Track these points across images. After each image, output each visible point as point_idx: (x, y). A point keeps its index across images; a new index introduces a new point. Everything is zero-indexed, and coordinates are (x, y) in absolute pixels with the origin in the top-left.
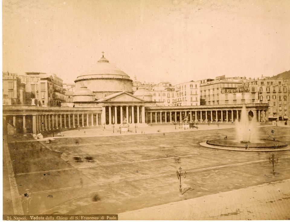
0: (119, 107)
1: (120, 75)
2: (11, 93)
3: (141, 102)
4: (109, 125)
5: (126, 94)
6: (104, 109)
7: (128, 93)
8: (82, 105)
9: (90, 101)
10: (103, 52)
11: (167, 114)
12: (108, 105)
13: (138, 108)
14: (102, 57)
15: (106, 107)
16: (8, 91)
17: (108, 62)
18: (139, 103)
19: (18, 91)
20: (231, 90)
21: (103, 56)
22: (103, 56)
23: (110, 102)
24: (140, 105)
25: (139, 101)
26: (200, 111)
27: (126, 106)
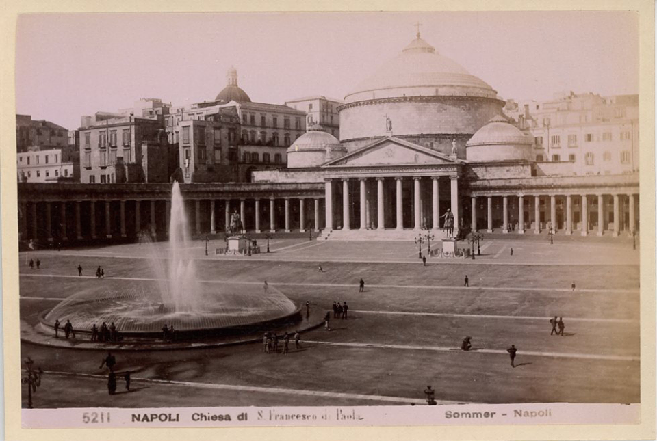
0: (371, 182)
1: (425, 86)
2: (126, 153)
3: (445, 165)
4: (360, 230)
5: (395, 143)
6: (328, 188)
7: (398, 140)
8: (292, 177)
9: (314, 165)
10: (418, 25)
11: (542, 202)
12: (337, 177)
13: (435, 184)
15: (332, 182)
16: (124, 150)
17: (431, 50)
19: (138, 149)
20: (329, 121)
21: (418, 35)
22: (418, 35)
23: (345, 169)
24: (441, 173)
25: (440, 162)
26: (534, 197)
27: (393, 178)
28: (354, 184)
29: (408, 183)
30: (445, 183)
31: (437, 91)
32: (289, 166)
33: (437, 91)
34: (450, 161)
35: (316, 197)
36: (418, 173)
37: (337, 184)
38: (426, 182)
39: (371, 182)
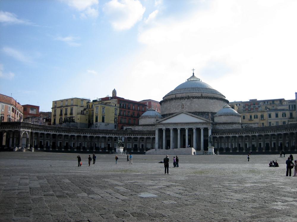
3: (205, 123)
6: (157, 132)
13: (202, 131)
14: (193, 75)
21: (193, 74)
22: (193, 74)
23: (164, 124)
24: (205, 126)
28: (168, 130)
29: (190, 130)
30: (206, 130)
31: (202, 94)
32: (140, 124)
33: (202, 94)
35: (152, 137)
36: (194, 127)
37: (161, 131)
38: (198, 130)
39: (175, 130)
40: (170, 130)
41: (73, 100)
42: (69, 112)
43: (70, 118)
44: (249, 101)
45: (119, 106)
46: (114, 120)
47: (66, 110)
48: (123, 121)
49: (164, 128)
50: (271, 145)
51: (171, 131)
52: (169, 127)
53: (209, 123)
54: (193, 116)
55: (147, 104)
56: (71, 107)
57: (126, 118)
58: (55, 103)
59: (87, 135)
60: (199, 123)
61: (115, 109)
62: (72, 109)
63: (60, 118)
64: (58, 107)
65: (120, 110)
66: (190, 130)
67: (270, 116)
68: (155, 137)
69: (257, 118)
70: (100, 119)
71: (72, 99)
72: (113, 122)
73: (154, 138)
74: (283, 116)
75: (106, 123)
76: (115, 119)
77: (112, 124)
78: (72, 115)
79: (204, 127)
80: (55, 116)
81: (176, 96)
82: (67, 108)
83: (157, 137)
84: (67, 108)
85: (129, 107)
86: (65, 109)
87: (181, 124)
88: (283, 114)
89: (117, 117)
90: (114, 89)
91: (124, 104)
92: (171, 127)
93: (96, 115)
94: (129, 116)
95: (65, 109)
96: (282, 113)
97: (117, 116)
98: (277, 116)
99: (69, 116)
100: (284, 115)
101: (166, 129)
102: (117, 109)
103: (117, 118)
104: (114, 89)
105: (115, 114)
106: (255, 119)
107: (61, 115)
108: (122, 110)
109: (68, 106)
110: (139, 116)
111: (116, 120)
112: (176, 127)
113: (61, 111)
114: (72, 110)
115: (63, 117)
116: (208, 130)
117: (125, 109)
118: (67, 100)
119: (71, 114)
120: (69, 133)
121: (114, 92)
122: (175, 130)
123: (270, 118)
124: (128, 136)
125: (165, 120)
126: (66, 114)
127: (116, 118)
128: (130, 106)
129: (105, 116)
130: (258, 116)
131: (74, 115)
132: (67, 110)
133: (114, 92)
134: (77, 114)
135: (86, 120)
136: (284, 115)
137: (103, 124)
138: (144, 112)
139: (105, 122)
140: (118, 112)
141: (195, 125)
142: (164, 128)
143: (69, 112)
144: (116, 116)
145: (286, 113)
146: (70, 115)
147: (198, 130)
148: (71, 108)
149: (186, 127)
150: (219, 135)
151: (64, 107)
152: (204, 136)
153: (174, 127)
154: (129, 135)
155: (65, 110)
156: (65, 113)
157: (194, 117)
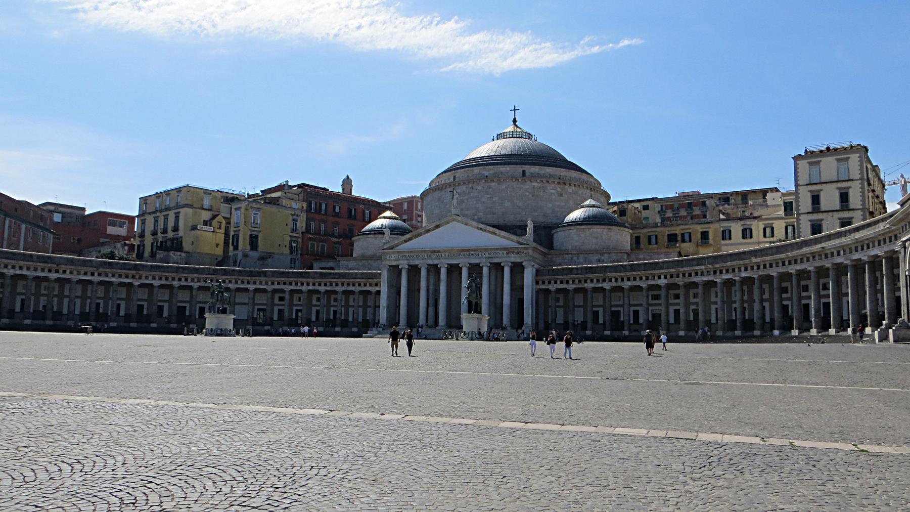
10: (515, 110)
18: (509, 251)
21: (515, 121)
22: (515, 121)
30: (517, 269)
34: (524, 244)
37: (395, 270)
40: (420, 269)
41: (181, 191)
42: (171, 224)
43: (172, 240)
44: (677, 195)
45: (305, 208)
46: (288, 246)
47: (166, 217)
48: (317, 247)
49: (404, 264)
50: (668, 315)
51: (423, 273)
52: (416, 262)
53: (526, 249)
54: (481, 229)
55: (405, 206)
56: (176, 211)
57: (323, 241)
58: (144, 201)
59: (191, 284)
60: (497, 249)
61: (293, 215)
62: (177, 215)
63: (152, 241)
64: (149, 214)
65: (309, 220)
66: (475, 270)
67: (726, 235)
68: (378, 289)
69: (690, 241)
70: (244, 244)
71: (179, 190)
72: (287, 251)
73: (378, 292)
74: (765, 236)
75: (263, 252)
76: (291, 242)
77: (282, 254)
78: (177, 233)
79: (513, 260)
80: (142, 236)
81: (454, 179)
82: (168, 215)
83: (384, 289)
84: (168, 215)
85: (337, 210)
86: (163, 218)
87: (451, 252)
88: (765, 230)
89: (299, 237)
90: (348, 176)
91: (321, 204)
92: (422, 263)
93: (234, 231)
94: (336, 234)
95: (164, 216)
96: (763, 226)
97: (300, 236)
98: (747, 233)
99: (170, 234)
100: (768, 231)
101: (409, 265)
102: (298, 216)
103: (300, 240)
104: (348, 176)
105: (294, 229)
106: (684, 245)
107: (154, 233)
108: (314, 220)
109: (168, 209)
110: (349, 236)
111: (294, 245)
112: (435, 262)
113: (156, 221)
114: (177, 217)
115: (160, 236)
116: (523, 267)
117: (324, 217)
118: (167, 193)
119: (176, 229)
120: (133, 277)
121: (347, 182)
122: (434, 269)
123: (728, 242)
124: (311, 287)
125: (406, 241)
126: (165, 231)
127: (293, 239)
128: (340, 207)
129: (260, 235)
130: (693, 237)
131: (181, 233)
132: (167, 219)
133: (347, 182)
134: (190, 228)
135: (217, 245)
136: (768, 231)
137: (254, 254)
138: (370, 222)
139: (260, 249)
140: (301, 225)
141: (487, 255)
142: (404, 264)
143: (171, 224)
144: (297, 235)
145: (774, 226)
146: (173, 231)
147: (497, 268)
148: (175, 213)
149: (463, 262)
150: (556, 283)
151: (161, 211)
152: (513, 289)
153: (430, 262)
154: (314, 284)
155: (164, 219)
156: (162, 227)
157: (485, 231)
